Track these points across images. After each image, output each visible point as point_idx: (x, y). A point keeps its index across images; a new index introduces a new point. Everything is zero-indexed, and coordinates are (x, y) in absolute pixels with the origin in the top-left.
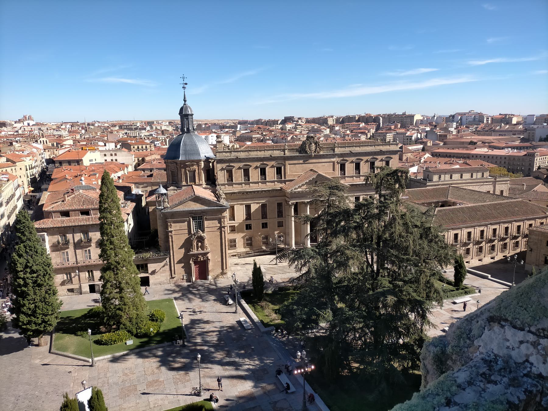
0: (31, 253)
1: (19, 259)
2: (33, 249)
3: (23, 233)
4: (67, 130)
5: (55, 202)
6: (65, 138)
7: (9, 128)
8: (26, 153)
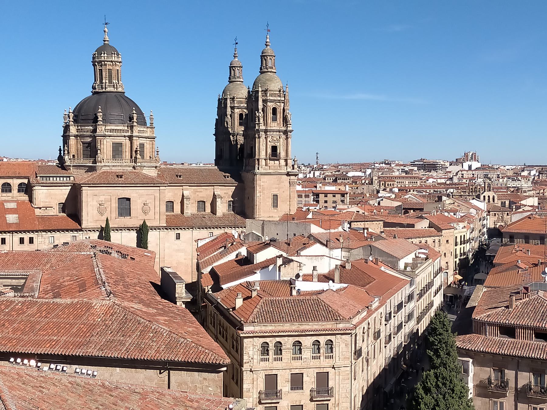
0: (444, 389)
1: (424, 395)
2: (448, 383)
3: (436, 352)
4: (531, 179)
5: (494, 306)
6: (525, 194)
7: (440, 173)
8: (459, 215)
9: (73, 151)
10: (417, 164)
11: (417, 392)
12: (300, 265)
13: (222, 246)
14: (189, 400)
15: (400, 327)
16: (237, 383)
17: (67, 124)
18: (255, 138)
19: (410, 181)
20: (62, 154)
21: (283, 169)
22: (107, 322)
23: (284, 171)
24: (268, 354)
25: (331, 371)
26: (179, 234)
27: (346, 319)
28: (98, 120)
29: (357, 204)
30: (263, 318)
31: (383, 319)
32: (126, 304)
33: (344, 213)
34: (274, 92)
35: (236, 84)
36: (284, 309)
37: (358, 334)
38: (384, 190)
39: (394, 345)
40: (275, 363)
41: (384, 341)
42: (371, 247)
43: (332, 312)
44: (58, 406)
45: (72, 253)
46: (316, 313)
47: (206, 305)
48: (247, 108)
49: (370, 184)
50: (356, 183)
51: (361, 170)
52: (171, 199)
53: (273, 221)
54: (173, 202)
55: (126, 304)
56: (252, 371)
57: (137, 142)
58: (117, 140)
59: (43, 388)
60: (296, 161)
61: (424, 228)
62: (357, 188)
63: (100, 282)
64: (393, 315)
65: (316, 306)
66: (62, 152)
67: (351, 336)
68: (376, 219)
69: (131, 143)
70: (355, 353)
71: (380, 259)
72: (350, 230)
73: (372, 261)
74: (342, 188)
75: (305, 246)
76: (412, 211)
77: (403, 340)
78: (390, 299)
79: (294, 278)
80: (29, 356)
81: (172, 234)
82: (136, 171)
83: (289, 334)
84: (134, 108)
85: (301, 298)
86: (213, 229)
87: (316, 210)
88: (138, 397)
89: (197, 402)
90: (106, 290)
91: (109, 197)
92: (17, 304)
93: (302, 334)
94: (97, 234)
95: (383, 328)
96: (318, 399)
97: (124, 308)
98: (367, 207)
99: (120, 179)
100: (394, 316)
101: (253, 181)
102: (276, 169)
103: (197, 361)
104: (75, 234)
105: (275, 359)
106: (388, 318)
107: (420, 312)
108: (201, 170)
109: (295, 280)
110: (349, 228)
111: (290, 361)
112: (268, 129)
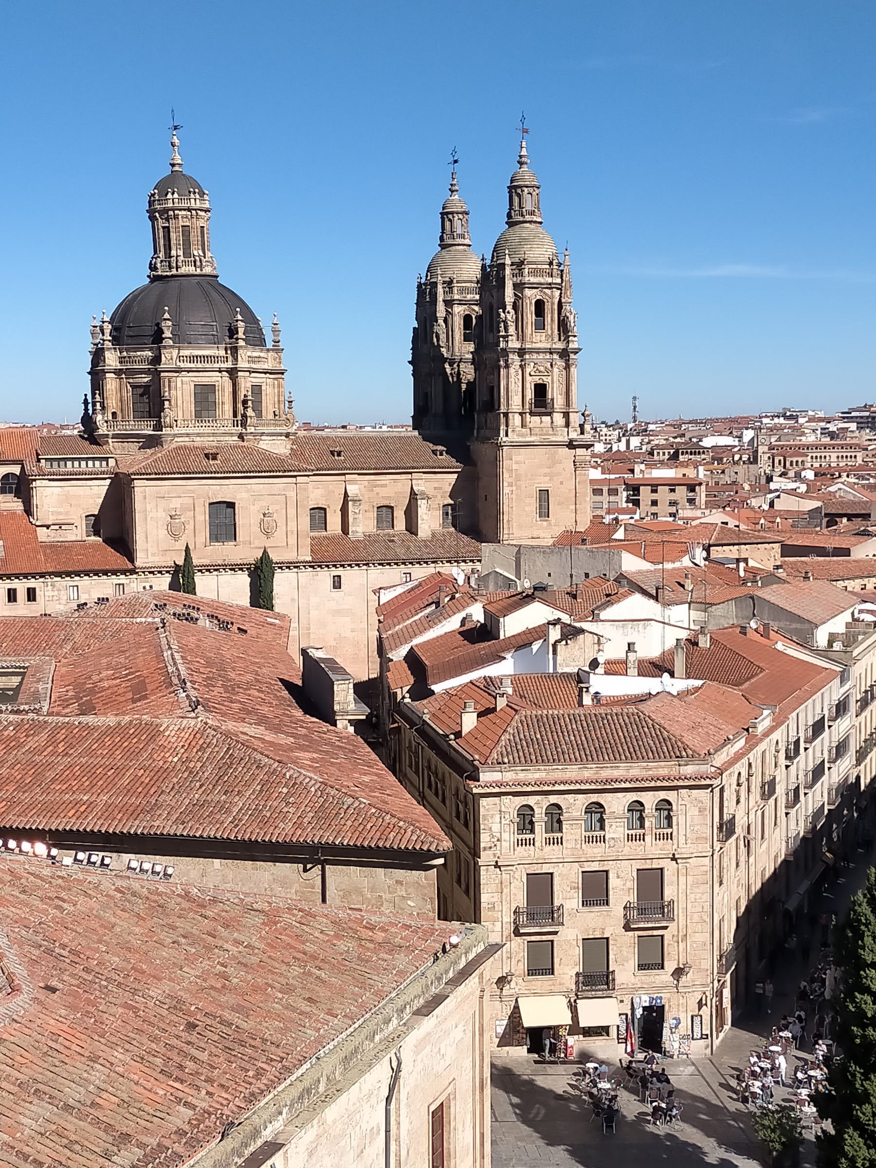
9: (112, 403)
10: (857, 417)
11: (855, 911)
12: (599, 639)
13: (431, 601)
14: (366, 927)
15: (818, 772)
16: (467, 892)
17: (99, 346)
18: (499, 367)
19: (840, 454)
20: (90, 412)
21: (560, 433)
22: (192, 765)
23: (563, 438)
24: (532, 831)
25: (669, 867)
26: (339, 576)
27: (700, 755)
28: (163, 336)
29: (724, 508)
30: (521, 754)
31: (782, 755)
32: (230, 725)
33: (695, 527)
34: (539, 266)
35: (456, 250)
36: (566, 734)
37: (726, 788)
38: (783, 475)
39: (806, 810)
40: (548, 848)
41: (784, 801)
42: (753, 600)
43: (670, 739)
44: (95, 938)
45: (117, 620)
46: (635, 744)
47: (399, 727)
48: (479, 303)
49: (751, 463)
50: (720, 461)
51: (731, 433)
52: (320, 502)
53: (539, 547)
54: (325, 509)
55: (230, 725)
56: (499, 867)
57: (246, 382)
58: (204, 379)
59: (64, 901)
60: (588, 416)
61: (871, 556)
62: (723, 472)
63: (175, 681)
64: (802, 745)
65: (635, 727)
66: (90, 407)
67: (712, 791)
68: (765, 538)
69: (235, 385)
70: (720, 828)
71: (775, 626)
72: (707, 563)
73: (756, 630)
74: (690, 473)
75: (610, 599)
76: (845, 520)
77: (826, 799)
78: (797, 711)
79: (587, 669)
80: (33, 835)
81: (325, 576)
82: (245, 444)
83: (578, 787)
84: (238, 309)
85: (602, 710)
86: (410, 566)
87: (632, 521)
88: (259, 920)
89: (383, 929)
90: (188, 696)
91: (191, 501)
92: (6, 728)
93: (605, 787)
94: (167, 578)
95: (780, 775)
96: (642, 925)
97: (227, 735)
98: (745, 513)
99: (211, 462)
100: (806, 749)
101: (495, 462)
102: (545, 435)
103: (381, 845)
104: (122, 580)
105: (548, 842)
106: (793, 752)
107: (863, 739)
108: (383, 440)
109: (589, 673)
110: (705, 559)
111: (579, 846)
112: (527, 346)
